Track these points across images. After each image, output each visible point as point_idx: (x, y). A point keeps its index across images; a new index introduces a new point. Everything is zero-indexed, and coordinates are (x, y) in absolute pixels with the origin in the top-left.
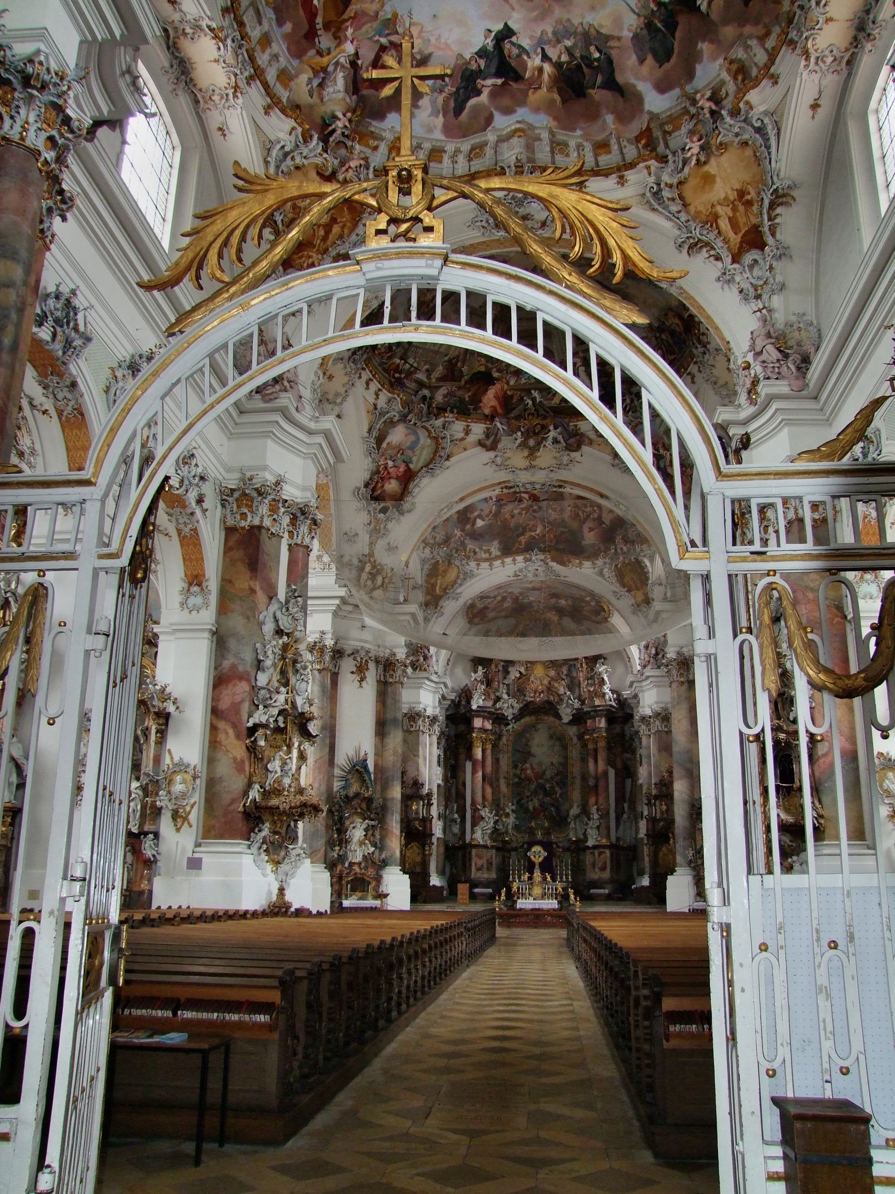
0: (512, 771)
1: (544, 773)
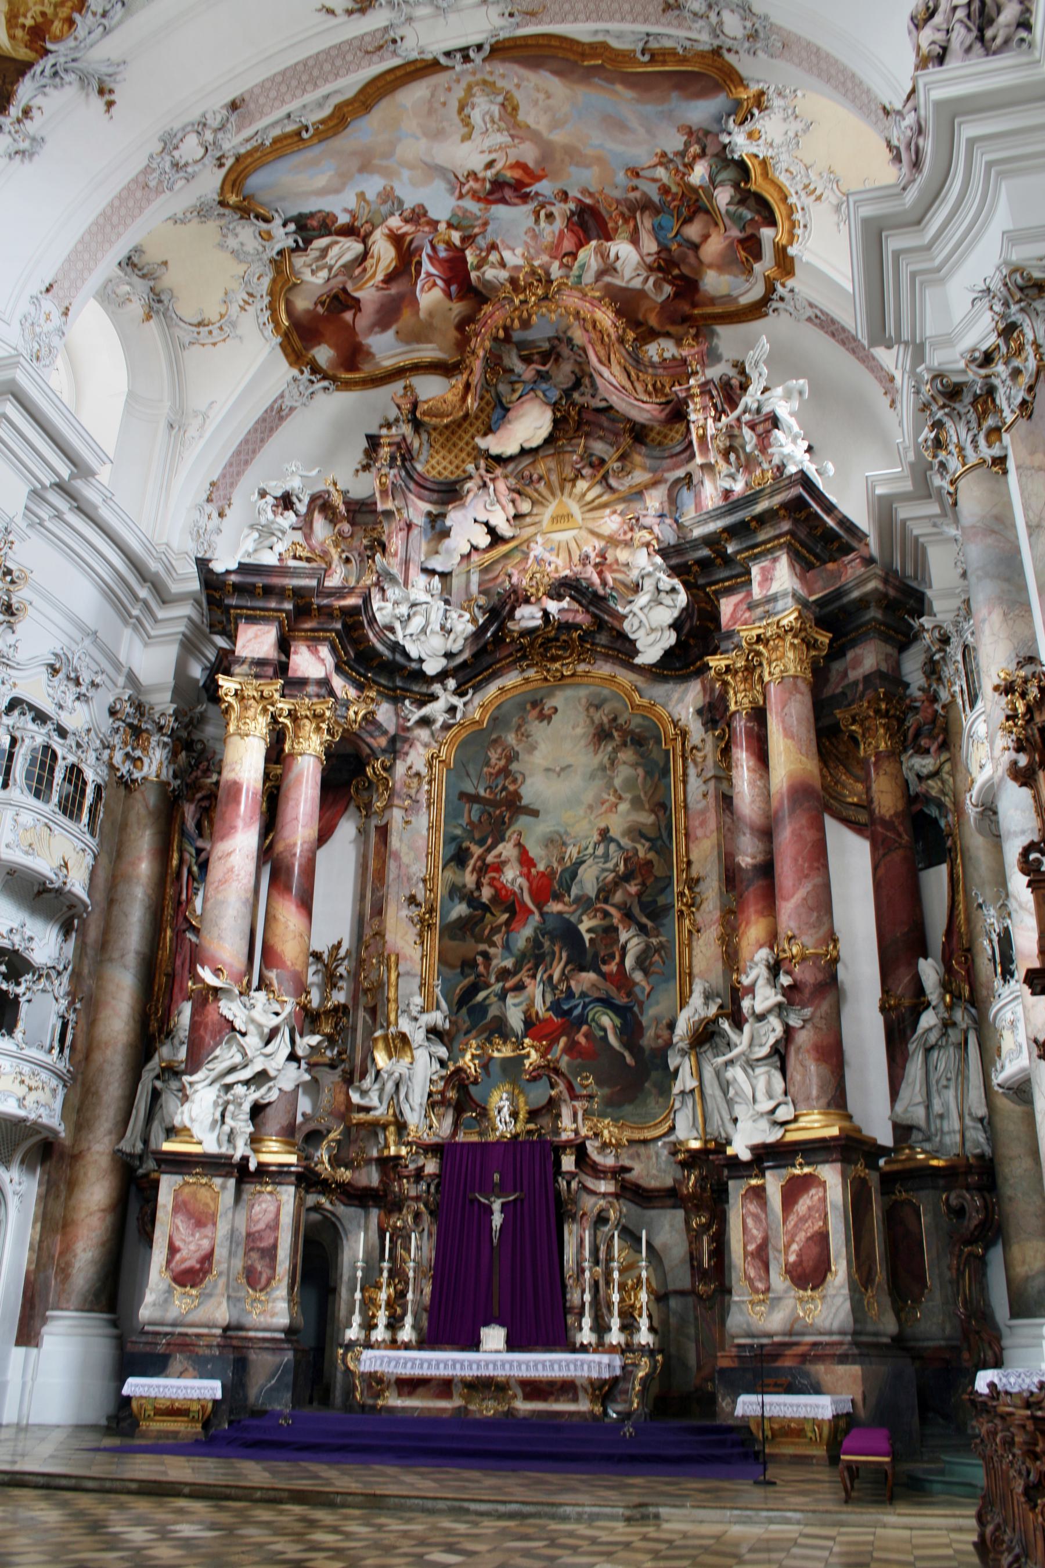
0: (444, 878)
1: (573, 872)
